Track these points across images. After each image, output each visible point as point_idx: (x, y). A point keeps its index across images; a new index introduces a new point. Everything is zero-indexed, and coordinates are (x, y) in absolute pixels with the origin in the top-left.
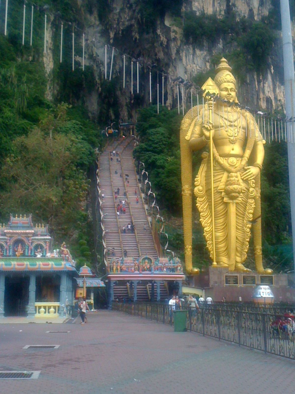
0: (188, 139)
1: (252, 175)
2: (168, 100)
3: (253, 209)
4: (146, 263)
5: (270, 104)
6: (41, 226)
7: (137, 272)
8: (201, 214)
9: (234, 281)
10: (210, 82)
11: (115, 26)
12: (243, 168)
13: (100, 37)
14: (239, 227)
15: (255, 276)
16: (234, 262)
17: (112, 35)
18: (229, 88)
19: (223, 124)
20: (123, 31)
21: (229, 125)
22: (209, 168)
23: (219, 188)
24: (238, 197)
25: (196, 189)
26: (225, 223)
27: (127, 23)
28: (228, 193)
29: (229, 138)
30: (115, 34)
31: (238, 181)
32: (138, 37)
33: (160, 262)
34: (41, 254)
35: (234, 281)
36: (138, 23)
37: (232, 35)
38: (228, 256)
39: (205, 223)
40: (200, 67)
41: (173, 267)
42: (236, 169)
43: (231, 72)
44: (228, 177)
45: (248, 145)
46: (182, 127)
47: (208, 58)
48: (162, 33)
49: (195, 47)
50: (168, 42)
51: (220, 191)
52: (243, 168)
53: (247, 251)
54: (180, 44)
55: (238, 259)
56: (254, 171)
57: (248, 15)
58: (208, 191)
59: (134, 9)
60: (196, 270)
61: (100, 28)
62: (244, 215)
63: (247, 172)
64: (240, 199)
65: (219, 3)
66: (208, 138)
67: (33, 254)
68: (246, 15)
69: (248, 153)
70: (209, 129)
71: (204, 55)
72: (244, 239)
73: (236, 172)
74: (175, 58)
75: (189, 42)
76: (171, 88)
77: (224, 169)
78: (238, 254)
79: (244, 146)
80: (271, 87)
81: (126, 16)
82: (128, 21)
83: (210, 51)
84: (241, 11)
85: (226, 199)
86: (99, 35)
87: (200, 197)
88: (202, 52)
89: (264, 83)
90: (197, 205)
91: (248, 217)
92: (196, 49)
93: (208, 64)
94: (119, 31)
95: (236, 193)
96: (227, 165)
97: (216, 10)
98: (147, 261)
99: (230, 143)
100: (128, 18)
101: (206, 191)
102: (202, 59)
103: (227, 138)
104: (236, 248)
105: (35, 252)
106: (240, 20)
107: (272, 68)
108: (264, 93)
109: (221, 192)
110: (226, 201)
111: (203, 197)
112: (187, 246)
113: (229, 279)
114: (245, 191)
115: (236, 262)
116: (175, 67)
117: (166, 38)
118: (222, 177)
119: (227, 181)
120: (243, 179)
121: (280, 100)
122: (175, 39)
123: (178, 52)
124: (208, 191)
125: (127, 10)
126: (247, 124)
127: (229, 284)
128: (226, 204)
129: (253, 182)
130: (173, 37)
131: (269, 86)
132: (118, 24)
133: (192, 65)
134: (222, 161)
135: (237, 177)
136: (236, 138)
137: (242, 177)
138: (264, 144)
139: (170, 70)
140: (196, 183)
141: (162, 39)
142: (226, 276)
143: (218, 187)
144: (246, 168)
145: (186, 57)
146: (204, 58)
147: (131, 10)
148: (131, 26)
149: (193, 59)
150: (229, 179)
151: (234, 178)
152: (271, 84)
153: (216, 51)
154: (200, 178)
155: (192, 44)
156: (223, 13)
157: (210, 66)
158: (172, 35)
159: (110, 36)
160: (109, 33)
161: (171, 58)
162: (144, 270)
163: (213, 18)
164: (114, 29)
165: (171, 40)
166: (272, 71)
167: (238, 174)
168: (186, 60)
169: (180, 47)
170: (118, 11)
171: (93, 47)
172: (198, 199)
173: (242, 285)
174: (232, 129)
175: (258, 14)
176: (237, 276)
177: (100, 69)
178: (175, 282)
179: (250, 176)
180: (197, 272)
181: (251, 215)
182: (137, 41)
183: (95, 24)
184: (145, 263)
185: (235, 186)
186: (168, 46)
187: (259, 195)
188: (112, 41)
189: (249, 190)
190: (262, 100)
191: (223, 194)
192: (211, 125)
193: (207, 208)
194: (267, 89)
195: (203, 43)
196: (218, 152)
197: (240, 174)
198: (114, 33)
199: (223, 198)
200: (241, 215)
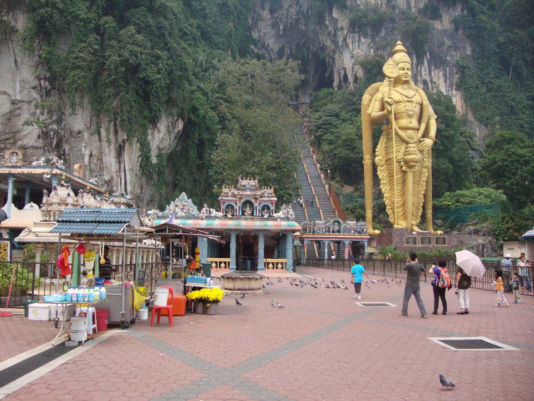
0: (369, 113)
2: (335, 82)
3: (426, 178)
4: (336, 226)
5: (426, 86)
6: (267, 188)
7: (327, 233)
8: (381, 181)
9: (413, 242)
10: (390, 62)
11: (284, 20)
12: (419, 140)
13: (271, 29)
14: (415, 194)
16: (410, 225)
17: (281, 28)
18: (406, 67)
19: (402, 100)
20: (291, 23)
22: (389, 139)
23: (398, 158)
24: (415, 166)
25: (377, 159)
26: (402, 191)
27: (294, 17)
28: (406, 162)
30: (284, 27)
31: (415, 151)
32: (304, 29)
34: (268, 215)
35: (413, 242)
36: (304, 17)
37: (393, 25)
38: (405, 218)
39: (385, 190)
40: (365, 53)
41: (359, 229)
43: (406, 53)
44: (407, 148)
45: (423, 120)
46: (363, 102)
47: (372, 45)
48: (330, 24)
50: (335, 32)
52: (419, 140)
53: (420, 215)
54: (347, 33)
55: (414, 222)
56: (429, 142)
57: (406, 8)
58: (389, 161)
59: (300, 5)
60: (377, 232)
61: (270, 22)
62: (419, 183)
63: (423, 143)
64: (417, 168)
66: (390, 112)
67: (260, 215)
68: (404, 8)
69: (423, 126)
71: (368, 42)
72: (419, 204)
73: (413, 143)
74: (341, 45)
76: (338, 71)
78: (414, 218)
79: (420, 121)
80: (427, 71)
81: (293, 11)
82: (295, 15)
83: (373, 39)
84: (400, 4)
85: (404, 168)
86: (270, 27)
87: (380, 166)
89: (421, 68)
90: (378, 173)
92: (361, 37)
93: (372, 50)
97: (378, 4)
98: (336, 223)
100: (295, 13)
101: (386, 161)
104: (413, 214)
105: (262, 212)
106: (400, 11)
107: (428, 54)
108: (421, 76)
109: (401, 161)
111: (383, 166)
112: (368, 211)
113: (409, 240)
115: (412, 225)
116: (341, 53)
117: (334, 28)
119: (406, 152)
120: (419, 150)
121: (435, 82)
122: (342, 29)
123: (345, 40)
124: (389, 161)
125: (295, 6)
126: (422, 100)
127: (409, 244)
128: (405, 172)
131: (425, 70)
132: (287, 17)
133: (358, 51)
134: (401, 133)
135: (414, 148)
137: (419, 148)
138: (436, 119)
139: (337, 55)
141: (330, 29)
142: (406, 237)
144: (422, 140)
145: (352, 43)
146: (369, 45)
147: (298, 6)
148: (298, 19)
149: (359, 45)
150: (407, 150)
151: (412, 149)
152: (427, 68)
153: (379, 38)
154: (380, 148)
155: (358, 32)
156: (384, 5)
157: (374, 52)
158: (339, 26)
159: (280, 28)
160: (279, 26)
161: (338, 45)
162: (333, 232)
163: (375, 10)
164: (283, 22)
165: (338, 30)
166: (428, 57)
168: (353, 46)
169: (346, 36)
170: (287, 7)
171: (265, 38)
172: (378, 167)
173: (421, 245)
174: (410, 104)
175: (415, 7)
176: (416, 238)
177: (271, 57)
178: (361, 243)
180: (379, 234)
181: (424, 183)
182: (304, 32)
183: (267, 18)
184: (334, 225)
185: (413, 156)
186: (335, 35)
187: (431, 165)
188: (281, 32)
189: (423, 160)
190: (419, 82)
191: (402, 163)
192: (392, 100)
193: (386, 176)
194: (423, 73)
196: (397, 125)
199: (402, 167)
200: (416, 182)
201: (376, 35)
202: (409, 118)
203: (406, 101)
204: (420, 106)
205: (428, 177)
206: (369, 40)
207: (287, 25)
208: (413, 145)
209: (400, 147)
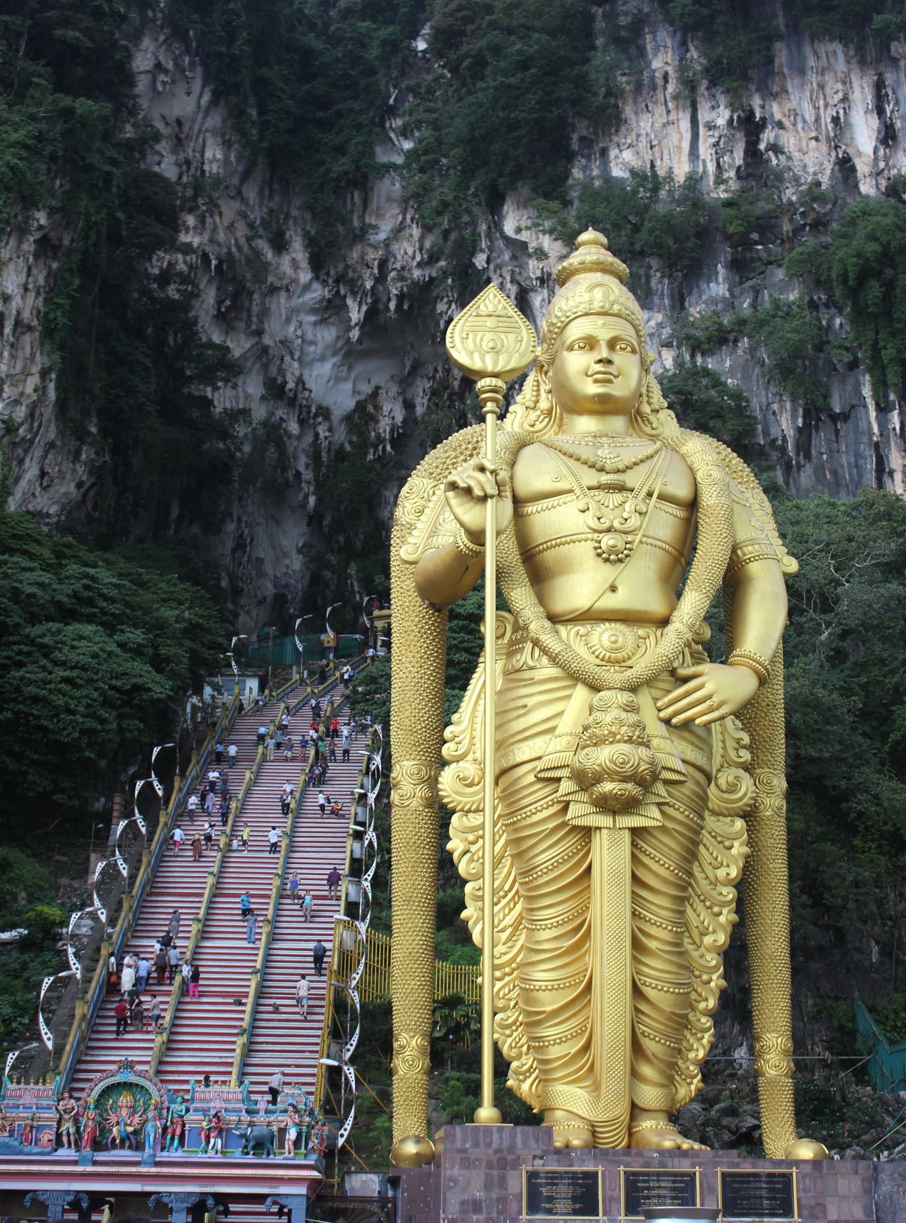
13: (315, 324)
20: (401, 298)
30: (372, 314)
42: (629, 673)
44: (591, 709)
73: (633, 689)
77: (574, 677)
82: (420, 265)
86: (312, 318)
94: (389, 300)
95: (625, 780)
100: (418, 258)
109: (559, 780)
119: (586, 728)
130: (539, 274)
132: (381, 279)
159: (350, 320)
191: (566, 786)
198: (364, 308)
207: (388, 309)
208: (624, 697)
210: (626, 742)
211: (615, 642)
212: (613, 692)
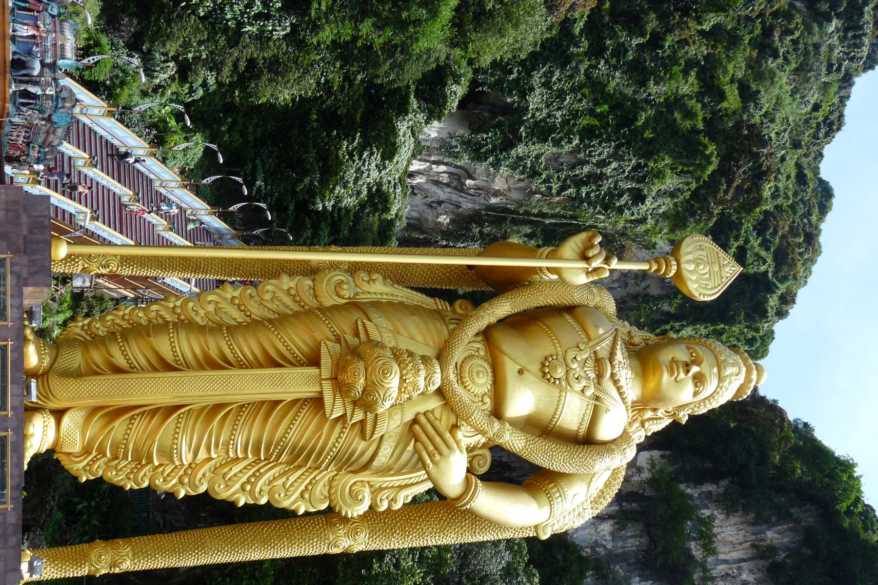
1: (438, 457)
3: (285, 504)
15: (5, 410)
21: (600, 356)
29: (557, 355)
33: (58, 22)
49: (615, 521)
51: (360, 328)
63: (448, 435)
65: (727, 574)
70: (590, 254)
71: (604, 543)
75: (624, 504)
88: (608, 538)
90: (285, 278)
91: (258, 478)
92: (611, 522)
96: (458, 354)
99: (543, 359)
102: (594, 538)
103: (556, 348)
110: (324, 350)
111: (316, 296)
114: (373, 434)
118: (412, 338)
120: (415, 421)
126: (604, 443)
129: (394, 500)
136: (563, 383)
137: (422, 419)
140: (364, 275)
143: (370, 320)
167: (434, 404)
179: (431, 448)
195: (631, 537)
196: (501, 321)
197: (432, 412)
201: (629, 564)
202: (540, 366)
203: (595, 352)
204: (583, 431)
205: (287, 515)
206: (609, 546)
209: (419, 338)
210: (401, 378)
211: (478, 374)
212: (439, 371)
